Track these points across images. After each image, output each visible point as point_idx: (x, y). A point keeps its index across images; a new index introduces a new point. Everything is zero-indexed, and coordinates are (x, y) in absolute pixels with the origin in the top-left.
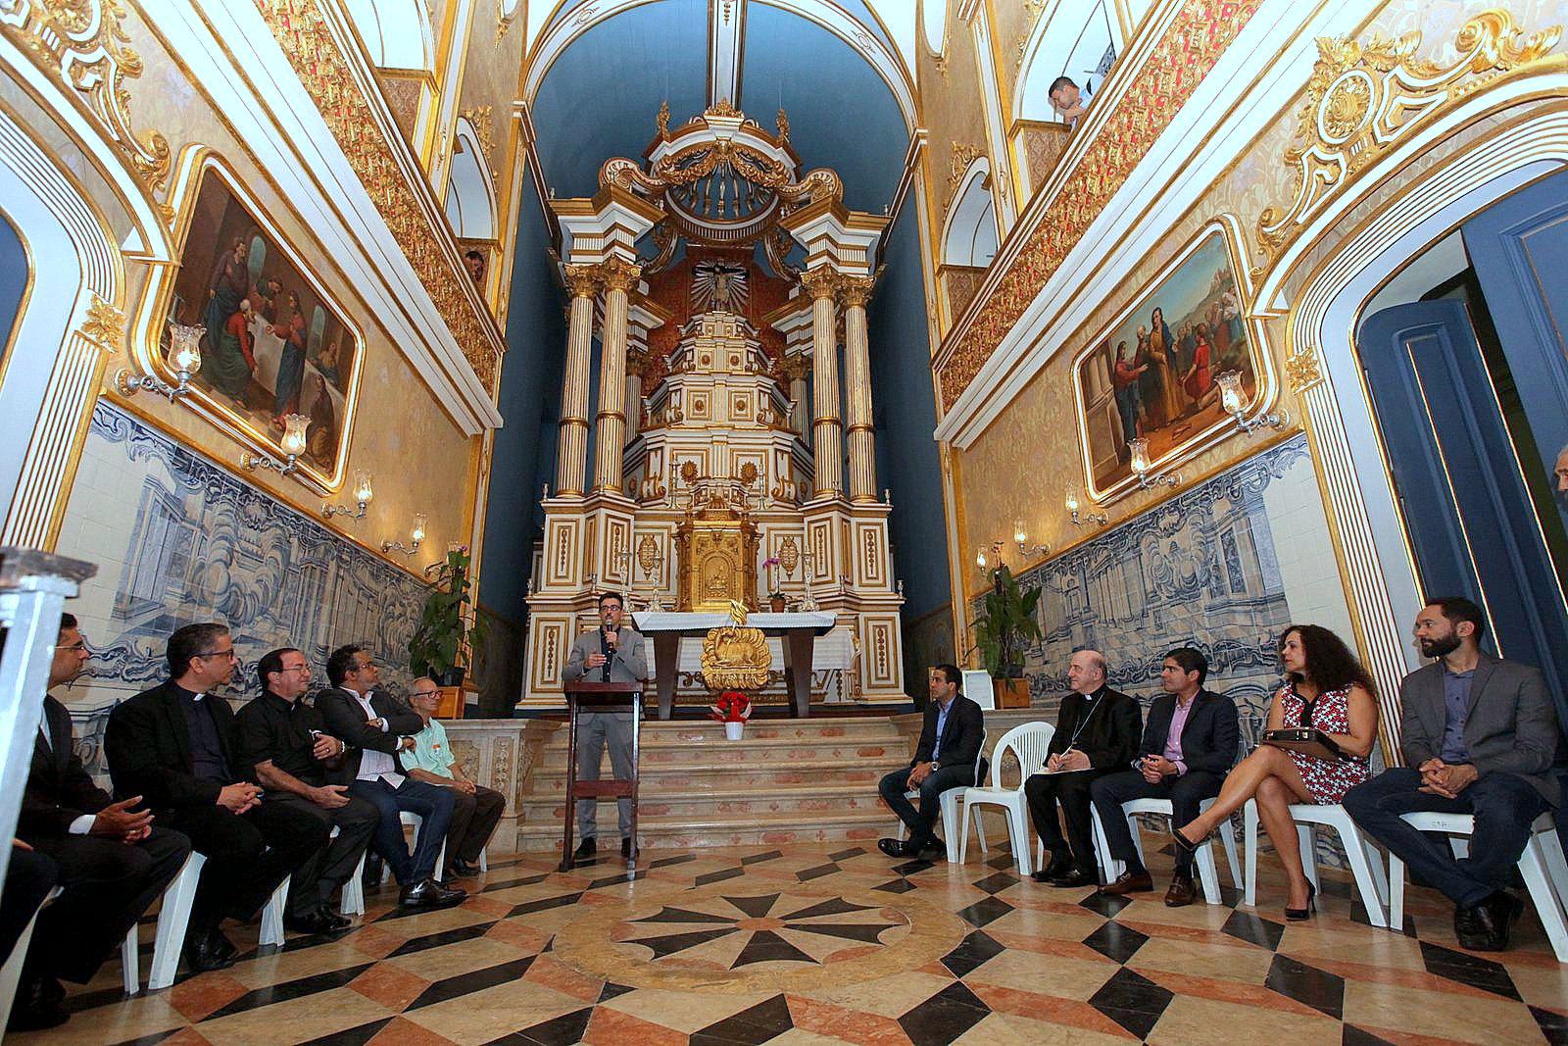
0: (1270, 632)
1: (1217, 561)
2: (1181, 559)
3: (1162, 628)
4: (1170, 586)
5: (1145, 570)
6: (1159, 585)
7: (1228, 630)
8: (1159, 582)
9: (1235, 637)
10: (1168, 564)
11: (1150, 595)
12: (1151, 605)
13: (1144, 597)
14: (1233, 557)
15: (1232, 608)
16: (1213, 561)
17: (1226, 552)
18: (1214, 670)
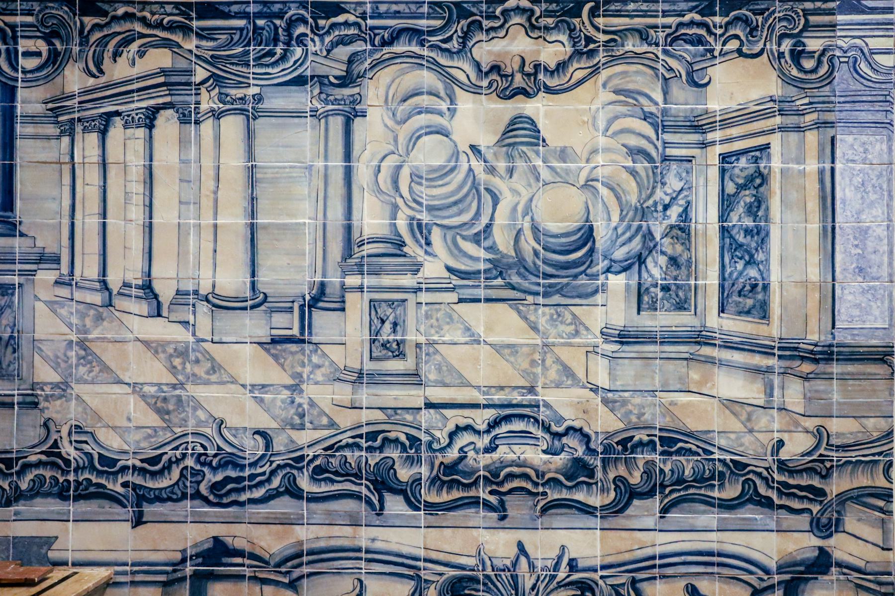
0: (820, 434)
1: (685, 215)
2: (545, 174)
3: (400, 354)
4: (476, 239)
5: (363, 173)
6: (420, 230)
7: (672, 403)
8: (425, 217)
9: (693, 425)
10: (482, 176)
11: (368, 249)
12: (368, 281)
13: (336, 250)
14: (749, 223)
15: (706, 351)
16: (674, 213)
17: (726, 203)
18: (596, 500)
